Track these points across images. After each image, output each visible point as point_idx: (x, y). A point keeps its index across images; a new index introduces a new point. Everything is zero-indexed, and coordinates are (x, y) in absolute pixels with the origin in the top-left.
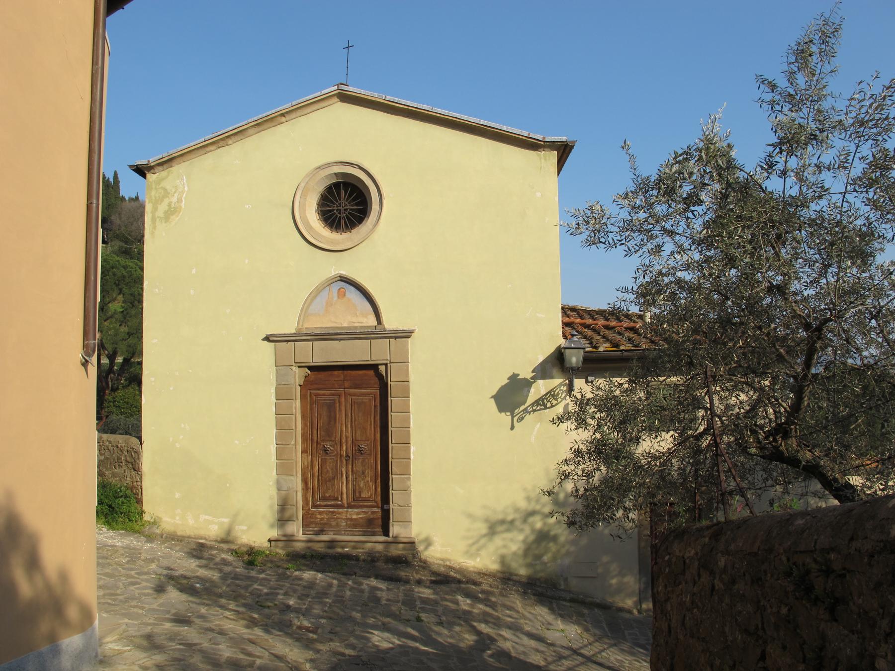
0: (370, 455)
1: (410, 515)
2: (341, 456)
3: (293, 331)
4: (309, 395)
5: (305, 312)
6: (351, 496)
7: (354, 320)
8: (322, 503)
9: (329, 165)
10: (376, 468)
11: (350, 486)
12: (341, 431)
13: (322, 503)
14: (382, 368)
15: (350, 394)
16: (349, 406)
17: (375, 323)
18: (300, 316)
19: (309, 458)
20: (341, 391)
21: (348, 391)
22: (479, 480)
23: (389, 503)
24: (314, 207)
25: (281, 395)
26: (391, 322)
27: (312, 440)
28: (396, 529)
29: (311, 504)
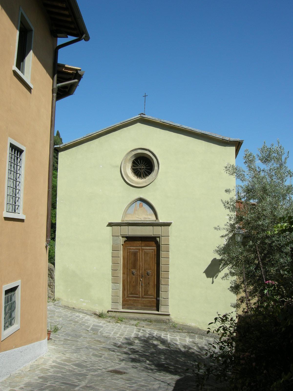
0: (152, 276)
1: (168, 303)
2: (140, 276)
3: (120, 221)
4: (126, 249)
5: (126, 213)
6: (143, 293)
7: (146, 217)
8: (131, 295)
9: (136, 149)
10: (154, 282)
11: (143, 289)
12: (140, 265)
13: (131, 295)
14: (158, 239)
15: (144, 249)
16: (143, 254)
17: (155, 219)
18: (123, 214)
19: (126, 276)
20: (140, 248)
21: (143, 248)
22: (202, 304)
23: (159, 297)
24: (130, 167)
25: (114, 249)
26: (161, 220)
27: (127, 268)
28: (162, 309)
29: (126, 296)
